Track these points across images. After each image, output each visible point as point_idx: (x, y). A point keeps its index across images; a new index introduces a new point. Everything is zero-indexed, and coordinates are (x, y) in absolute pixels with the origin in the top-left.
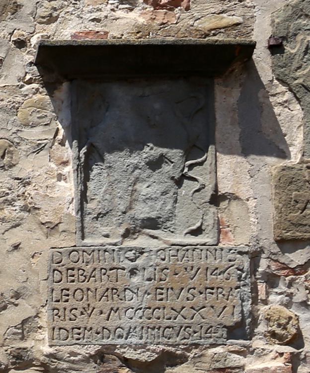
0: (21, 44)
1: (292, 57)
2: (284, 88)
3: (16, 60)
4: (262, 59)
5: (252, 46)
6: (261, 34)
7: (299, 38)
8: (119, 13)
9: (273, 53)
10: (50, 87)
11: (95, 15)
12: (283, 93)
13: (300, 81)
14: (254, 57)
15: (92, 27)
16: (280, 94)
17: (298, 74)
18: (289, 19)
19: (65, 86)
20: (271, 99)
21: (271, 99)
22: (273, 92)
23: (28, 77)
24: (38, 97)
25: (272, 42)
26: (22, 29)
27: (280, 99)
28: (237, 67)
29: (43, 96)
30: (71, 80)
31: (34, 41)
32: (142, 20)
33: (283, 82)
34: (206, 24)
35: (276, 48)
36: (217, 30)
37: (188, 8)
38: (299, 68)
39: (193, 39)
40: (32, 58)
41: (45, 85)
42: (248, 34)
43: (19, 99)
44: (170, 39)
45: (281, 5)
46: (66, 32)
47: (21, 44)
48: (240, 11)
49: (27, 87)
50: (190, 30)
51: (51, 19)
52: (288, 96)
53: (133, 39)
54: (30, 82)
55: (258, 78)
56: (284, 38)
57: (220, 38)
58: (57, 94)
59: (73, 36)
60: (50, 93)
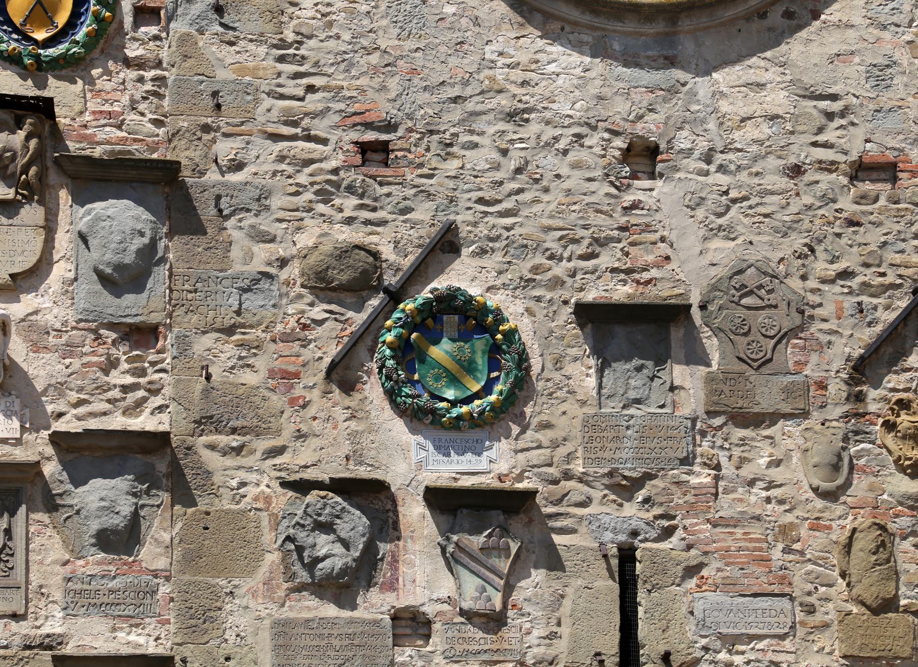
0: (566, 302)
1: (712, 312)
2: (707, 329)
4: (696, 313)
5: (690, 306)
6: (695, 299)
7: (716, 302)
8: (618, 287)
10: (582, 326)
11: (605, 288)
15: (604, 294)
16: (706, 332)
18: (710, 291)
19: (590, 326)
26: (566, 295)
27: (706, 335)
29: (578, 331)
30: (593, 323)
31: (573, 301)
32: (630, 291)
33: (707, 326)
34: (665, 294)
35: (703, 307)
36: (671, 297)
37: (655, 285)
39: (658, 302)
40: (571, 310)
41: (579, 325)
42: (688, 299)
45: (705, 284)
46: (590, 296)
47: (566, 302)
48: (683, 287)
50: (656, 296)
51: (581, 290)
52: (710, 333)
53: (626, 301)
54: (570, 323)
55: (694, 323)
57: (673, 301)
58: (585, 330)
59: (594, 299)
60: (582, 329)
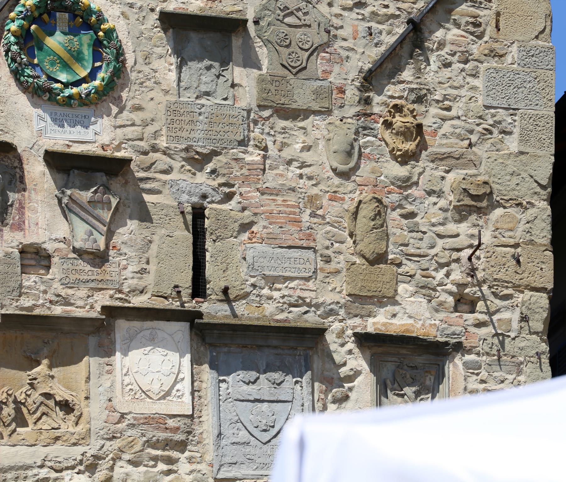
0: (152, 10)
1: (263, 27)
2: (259, 40)
3: (150, 17)
4: (250, 26)
5: (246, 21)
6: (250, 16)
7: (266, 19)
9: (255, 25)
10: (165, 30)
12: (260, 42)
13: (266, 38)
14: (248, 25)
16: (258, 43)
17: (265, 34)
18: (261, 10)
19: (171, 30)
20: (255, 44)
21: (255, 44)
22: (255, 41)
23: (156, 25)
24: (160, 34)
25: (255, 20)
27: (259, 45)
28: (241, 28)
29: (162, 34)
30: (173, 28)
31: (158, 9)
32: (202, 5)
33: (259, 38)
34: (228, 9)
35: (256, 23)
36: (232, 12)
38: (266, 32)
39: (223, 15)
40: (157, 17)
41: (163, 29)
43: (152, 34)
44: (214, 14)
45: (258, 4)
46: (171, 7)
47: (152, 10)
48: (241, 5)
49: (155, 29)
50: (222, 11)
52: (261, 43)
53: (199, 13)
54: (156, 27)
55: (249, 35)
56: (259, 18)
57: (234, 16)
58: (167, 33)
60: (165, 33)
